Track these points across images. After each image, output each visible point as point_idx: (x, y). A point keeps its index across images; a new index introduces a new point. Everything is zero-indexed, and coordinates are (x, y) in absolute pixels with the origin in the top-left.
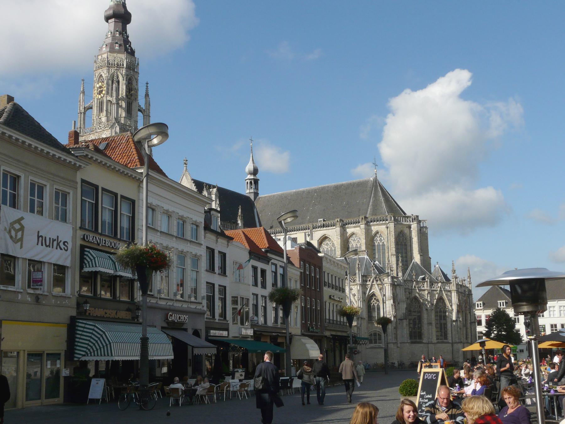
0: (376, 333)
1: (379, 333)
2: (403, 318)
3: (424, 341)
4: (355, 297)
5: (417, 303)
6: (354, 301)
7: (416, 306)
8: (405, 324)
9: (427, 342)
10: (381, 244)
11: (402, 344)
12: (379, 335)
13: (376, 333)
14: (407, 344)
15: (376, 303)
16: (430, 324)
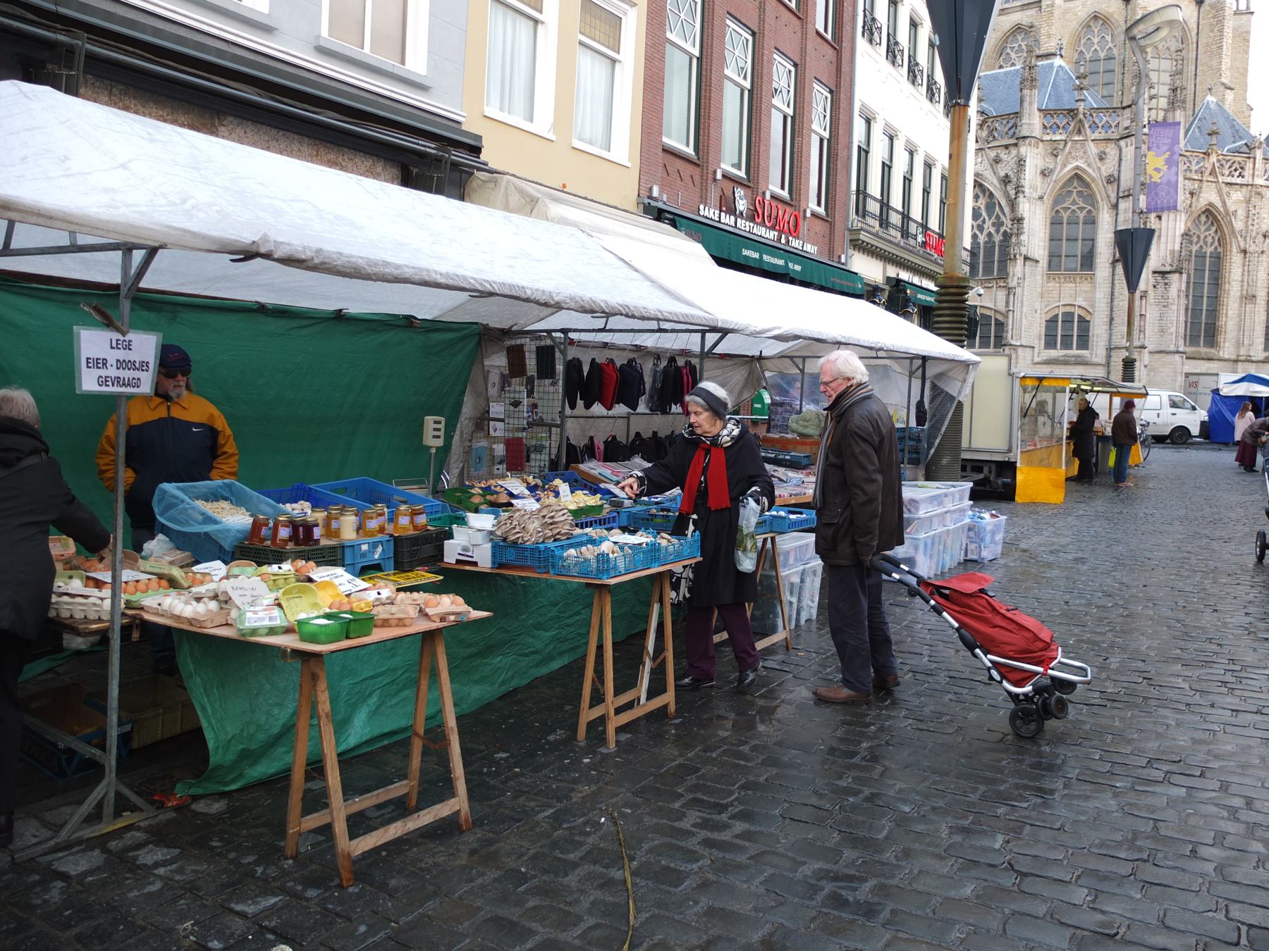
0: (1072, 314)
1: (1083, 313)
2: (1168, 268)
3: (1221, 354)
4: (1009, 188)
5: (1213, 229)
6: (1003, 203)
7: (1209, 240)
8: (1173, 291)
9: (1233, 357)
10: (1102, 55)
11: (1157, 356)
12: (1082, 320)
13: (1073, 313)
14: (1177, 357)
15: (1081, 209)
16: (1249, 298)
